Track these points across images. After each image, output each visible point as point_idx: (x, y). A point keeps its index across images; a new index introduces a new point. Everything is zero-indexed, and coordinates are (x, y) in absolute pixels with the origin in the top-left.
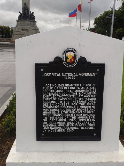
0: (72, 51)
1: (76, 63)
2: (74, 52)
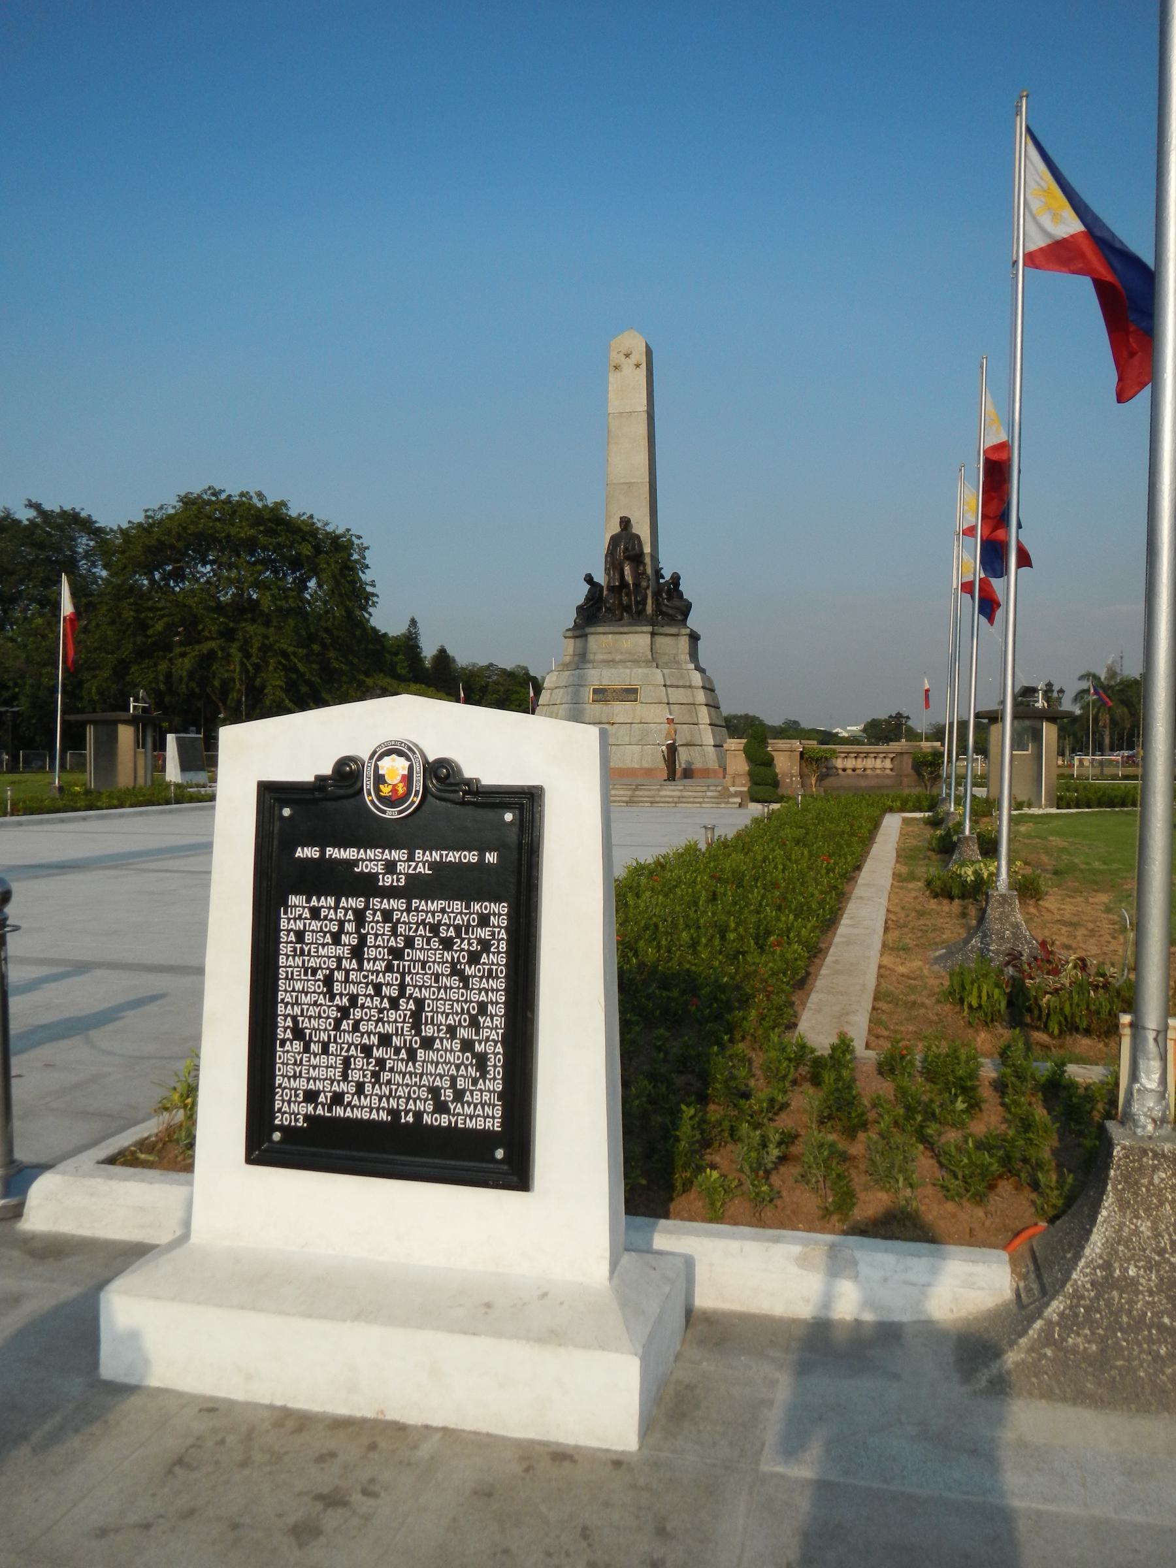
0: (400, 754)
1: (413, 802)
2: (408, 759)
